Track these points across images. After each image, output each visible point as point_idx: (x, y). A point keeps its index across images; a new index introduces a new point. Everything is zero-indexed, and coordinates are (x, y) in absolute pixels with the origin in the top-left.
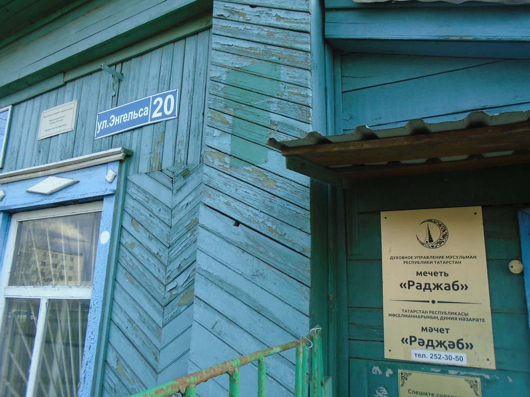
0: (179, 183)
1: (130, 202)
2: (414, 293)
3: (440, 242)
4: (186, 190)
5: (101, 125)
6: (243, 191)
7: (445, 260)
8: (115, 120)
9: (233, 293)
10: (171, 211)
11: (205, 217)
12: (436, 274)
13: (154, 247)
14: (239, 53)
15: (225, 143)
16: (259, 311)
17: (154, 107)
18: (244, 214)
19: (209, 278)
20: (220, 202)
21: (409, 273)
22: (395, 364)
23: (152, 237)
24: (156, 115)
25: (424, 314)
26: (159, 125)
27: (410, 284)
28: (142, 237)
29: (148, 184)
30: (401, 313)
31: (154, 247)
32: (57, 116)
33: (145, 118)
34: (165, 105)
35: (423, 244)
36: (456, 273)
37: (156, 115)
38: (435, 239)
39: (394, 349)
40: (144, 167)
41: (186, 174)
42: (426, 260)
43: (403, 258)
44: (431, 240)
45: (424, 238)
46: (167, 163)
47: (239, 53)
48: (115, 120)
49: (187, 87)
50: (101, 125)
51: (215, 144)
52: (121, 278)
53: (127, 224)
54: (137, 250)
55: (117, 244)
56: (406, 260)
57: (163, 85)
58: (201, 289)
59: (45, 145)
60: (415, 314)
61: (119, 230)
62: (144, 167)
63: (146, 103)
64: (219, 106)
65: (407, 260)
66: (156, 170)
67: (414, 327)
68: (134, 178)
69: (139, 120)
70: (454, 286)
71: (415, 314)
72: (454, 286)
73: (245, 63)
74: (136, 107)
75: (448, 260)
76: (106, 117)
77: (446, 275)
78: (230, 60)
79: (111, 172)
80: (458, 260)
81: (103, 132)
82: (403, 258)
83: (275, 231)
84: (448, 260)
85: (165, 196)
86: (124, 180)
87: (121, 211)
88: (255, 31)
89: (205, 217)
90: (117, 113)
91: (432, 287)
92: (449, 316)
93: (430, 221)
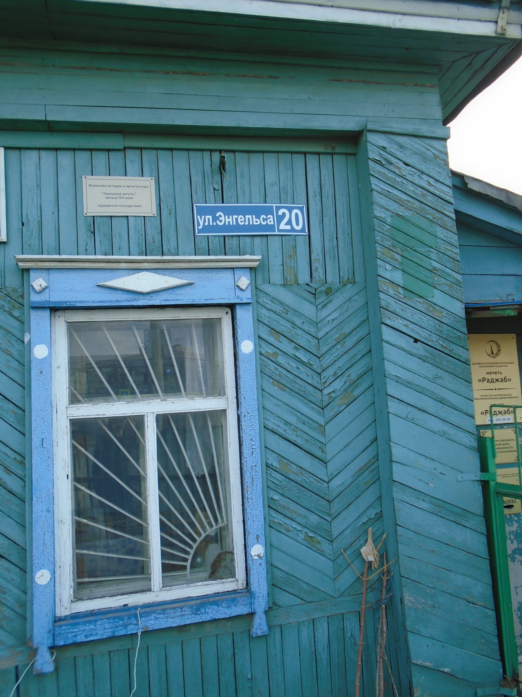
0: (322, 299)
2: (486, 385)
3: (497, 354)
4: (331, 307)
5: (202, 221)
6: (417, 317)
7: (500, 365)
8: (224, 220)
9: (421, 391)
12: (496, 373)
15: (398, 277)
16: (442, 401)
17: (280, 219)
18: (422, 335)
19: (398, 380)
20: (399, 323)
23: (299, 347)
24: (283, 226)
25: (491, 397)
27: (484, 379)
28: (288, 348)
29: (285, 296)
30: (480, 397)
32: (123, 193)
33: (271, 228)
34: (291, 219)
35: (489, 355)
37: (283, 226)
38: (495, 353)
40: (276, 277)
41: (329, 292)
42: (491, 365)
43: (479, 364)
44: (493, 353)
45: (489, 352)
48: (224, 220)
50: (202, 221)
51: (388, 275)
54: (281, 359)
56: (480, 365)
57: (285, 197)
58: (392, 389)
60: (487, 397)
62: (276, 277)
63: (269, 211)
64: (388, 244)
69: (260, 227)
71: (487, 397)
73: (407, 214)
74: (257, 212)
75: (501, 365)
76: (212, 211)
77: (501, 373)
78: (393, 206)
80: (506, 365)
81: (206, 229)
82: (479, 364)
83: (444, 347)
84: (501, 365)
88: (411, 187)
90: (228, 212)
91: (495, 380)
92: (503, 397)
93: (492, 341)
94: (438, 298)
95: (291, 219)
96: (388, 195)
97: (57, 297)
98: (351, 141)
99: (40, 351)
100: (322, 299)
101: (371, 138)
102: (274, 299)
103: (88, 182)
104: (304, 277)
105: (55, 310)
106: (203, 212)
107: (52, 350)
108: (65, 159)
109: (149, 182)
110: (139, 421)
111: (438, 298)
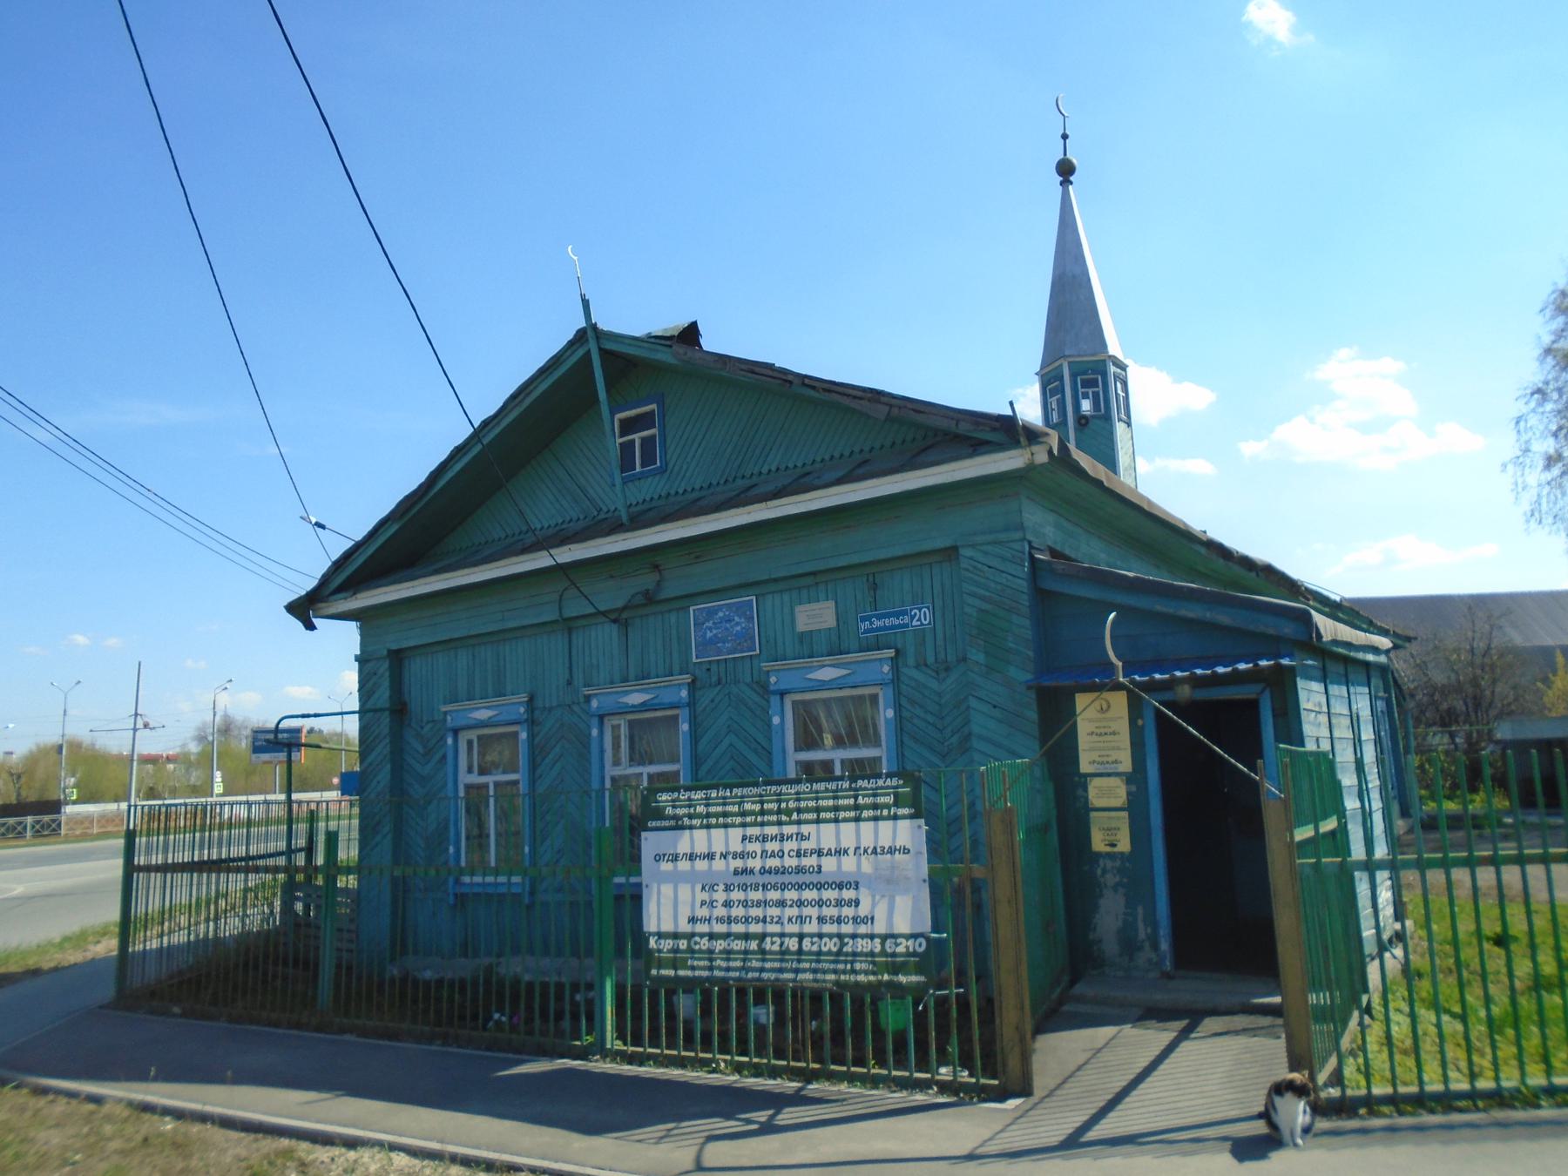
0: (943, 675)
1: (903, 687)
4: (949, 681)
5: (864, 626)
8: (877, 623)
10: (939, 695)
11: (973, 703)
13: (930, 718)
14: (983, 598)
15: (981, 658)
17: (913, 618)
21: (1091, 727)
22: (1086, 775)
26: (920, 633)
28: (919, 712)
31: (930, 718)
32: (817, 615)
33: (906, 626)
34: (922, 617)
36: (1114, 726)
39: (1085, 767)
40: (911, 661)
41: (947, 669)
46: (930, 660)
47: (983, 598)
48: (877, 623)
49: (938, 603)
50: (864, 626)
52: (906, 739)
53: (904, 702)
54: (916, 721)
55: (899, 716)
57: (918, 601)
59: (805, 638)
61: (898, 708)
63: (904, 613)
65: (1090, 720)
66: (921, 664)
67: (1095, 756)
68: (904, 670)
69: (900, 626)
70: (1114, 733)
72: (1114, 733)
74: (897, 615)
76: (868, 619)
78: (977, 602)
79: (886, 669)
81: (866, 631)
85: (934, 684)
86: (895, 668)
87: (898, 694)
89: (973, 703)
90: (879, 617)
94: (1013, 672)
95: (922, 617)
96: (974, 595)
97: (782, 687)
98: (951, 553)
99: (776, 720)
100: (943, 675)
101: (966, 552)
102: (911, 678)
103: (798, 609)
104: (930, 660)
105: (782, 694)
106: (863, 619)
107: (784, 721)
108: (786, 597)
109: (831, 604)
110: (832, 761)
111: (1013, 672)
